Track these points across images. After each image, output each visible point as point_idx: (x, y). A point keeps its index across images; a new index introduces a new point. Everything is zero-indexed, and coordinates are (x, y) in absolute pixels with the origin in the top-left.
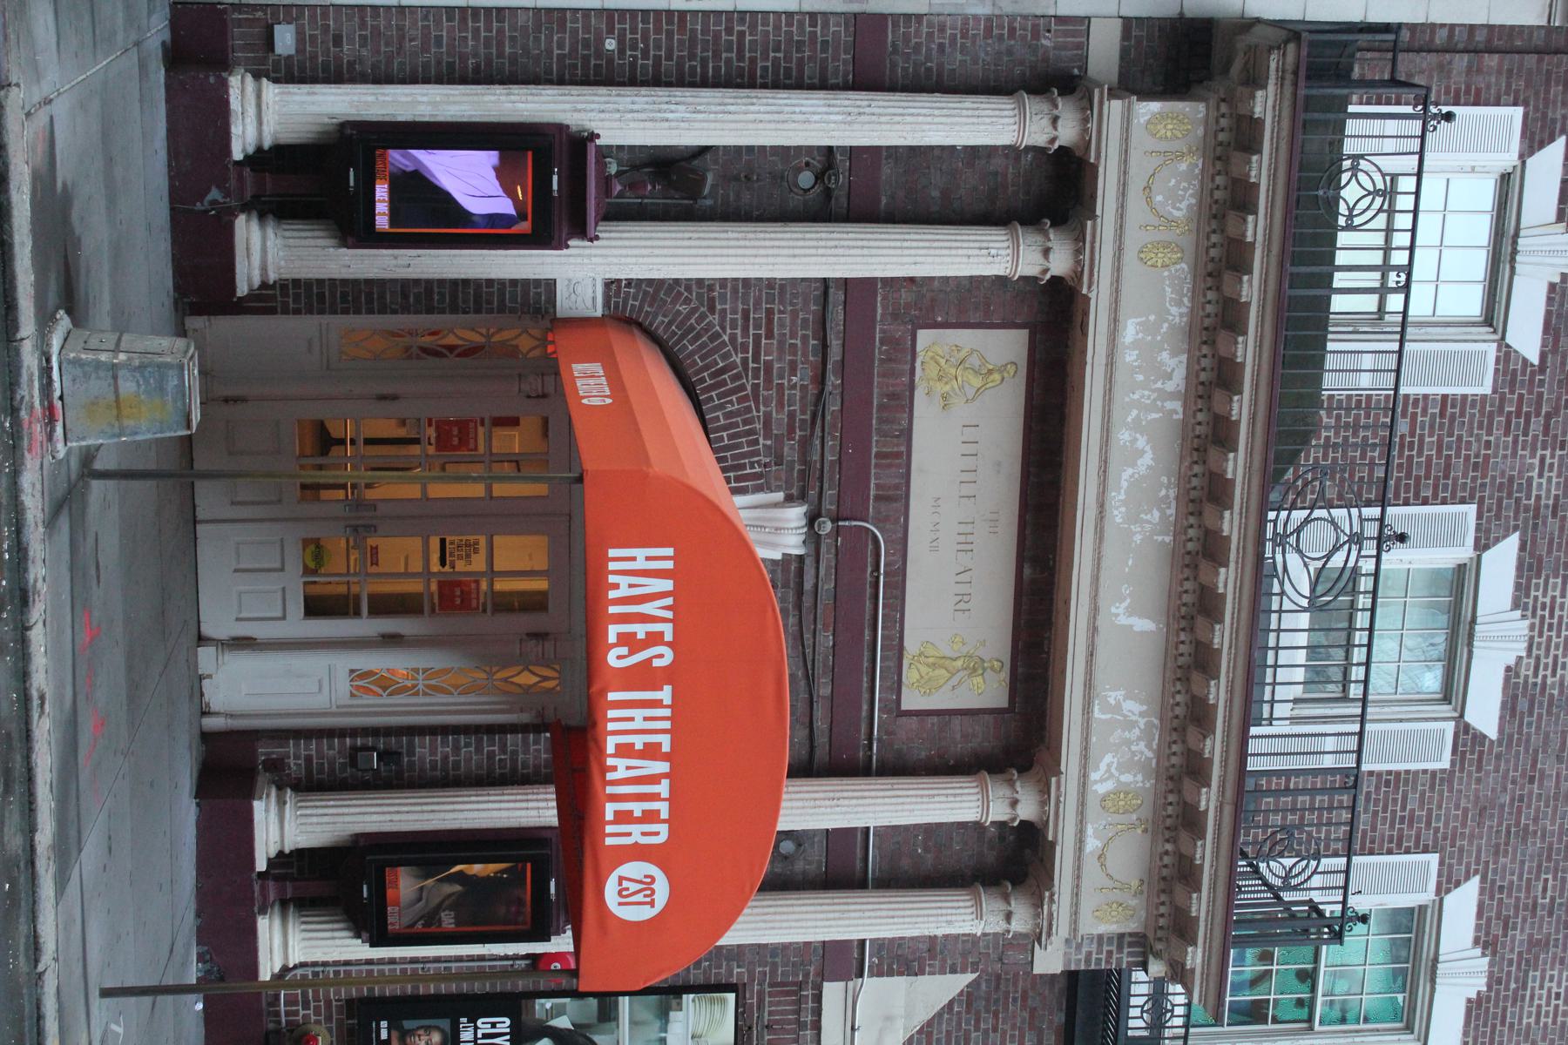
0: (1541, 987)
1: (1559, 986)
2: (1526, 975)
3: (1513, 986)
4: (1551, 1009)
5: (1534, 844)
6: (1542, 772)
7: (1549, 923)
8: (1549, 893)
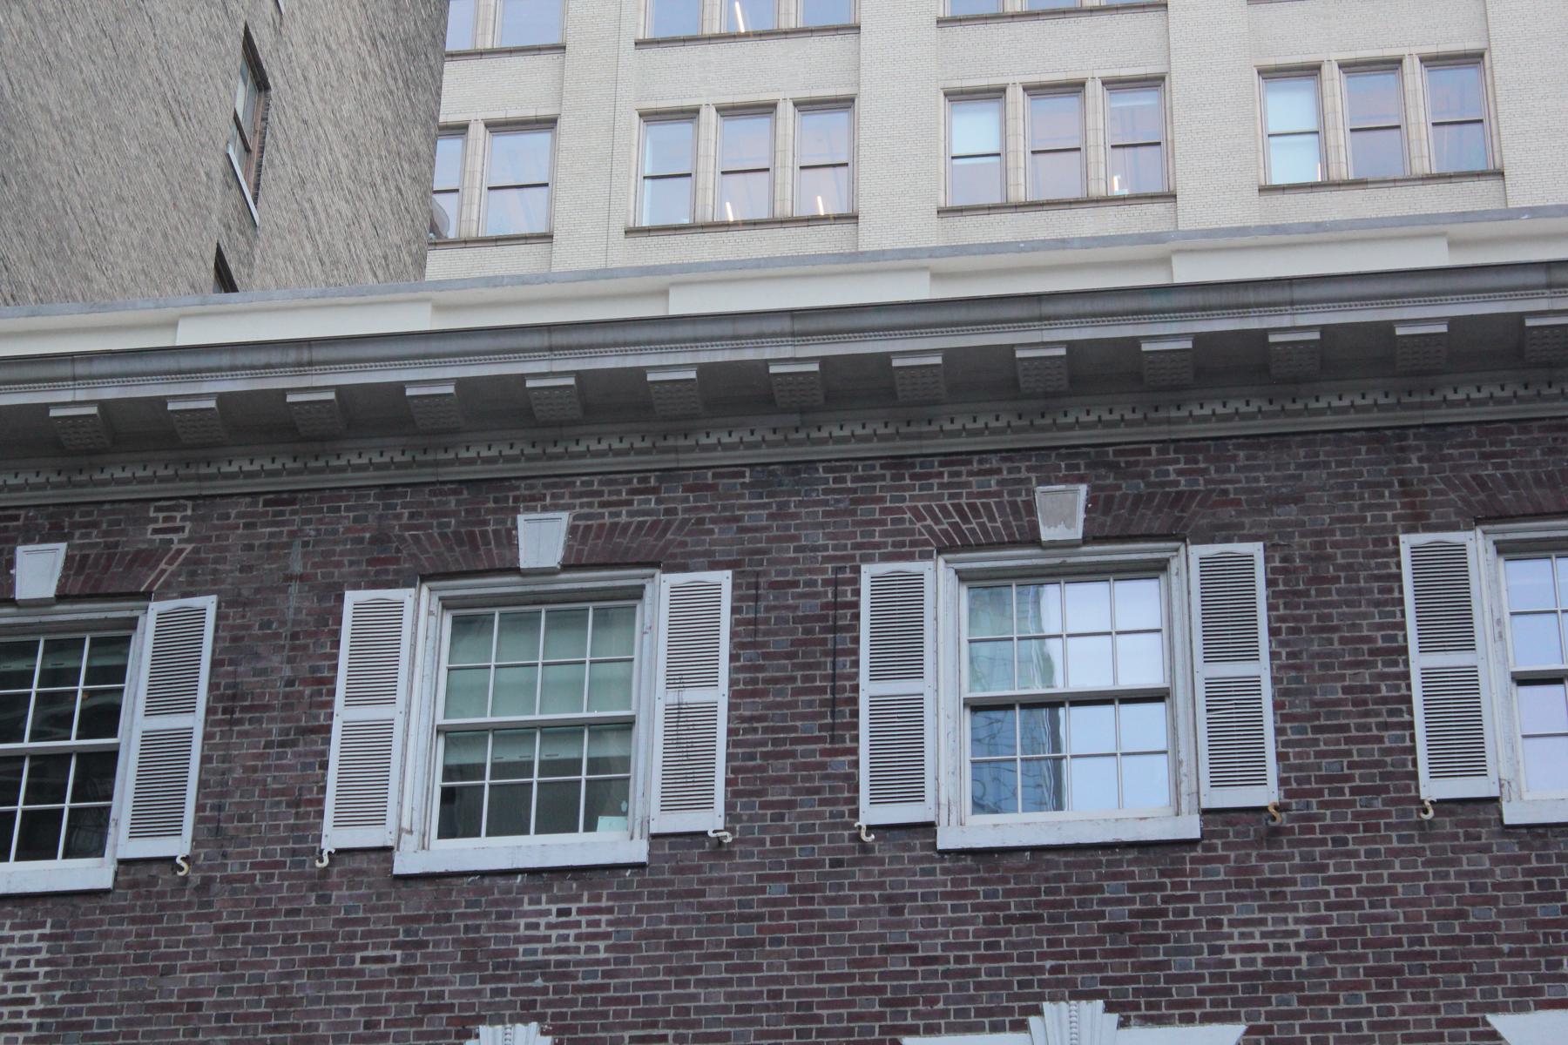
0: (547, 939)
1: (547, 913)
2: (524, 965)
3: (539, 982)
4: (584, 919)
5: (301, 987)
6: (184, 993)
7: (437, 944)
8: (387, 952)
